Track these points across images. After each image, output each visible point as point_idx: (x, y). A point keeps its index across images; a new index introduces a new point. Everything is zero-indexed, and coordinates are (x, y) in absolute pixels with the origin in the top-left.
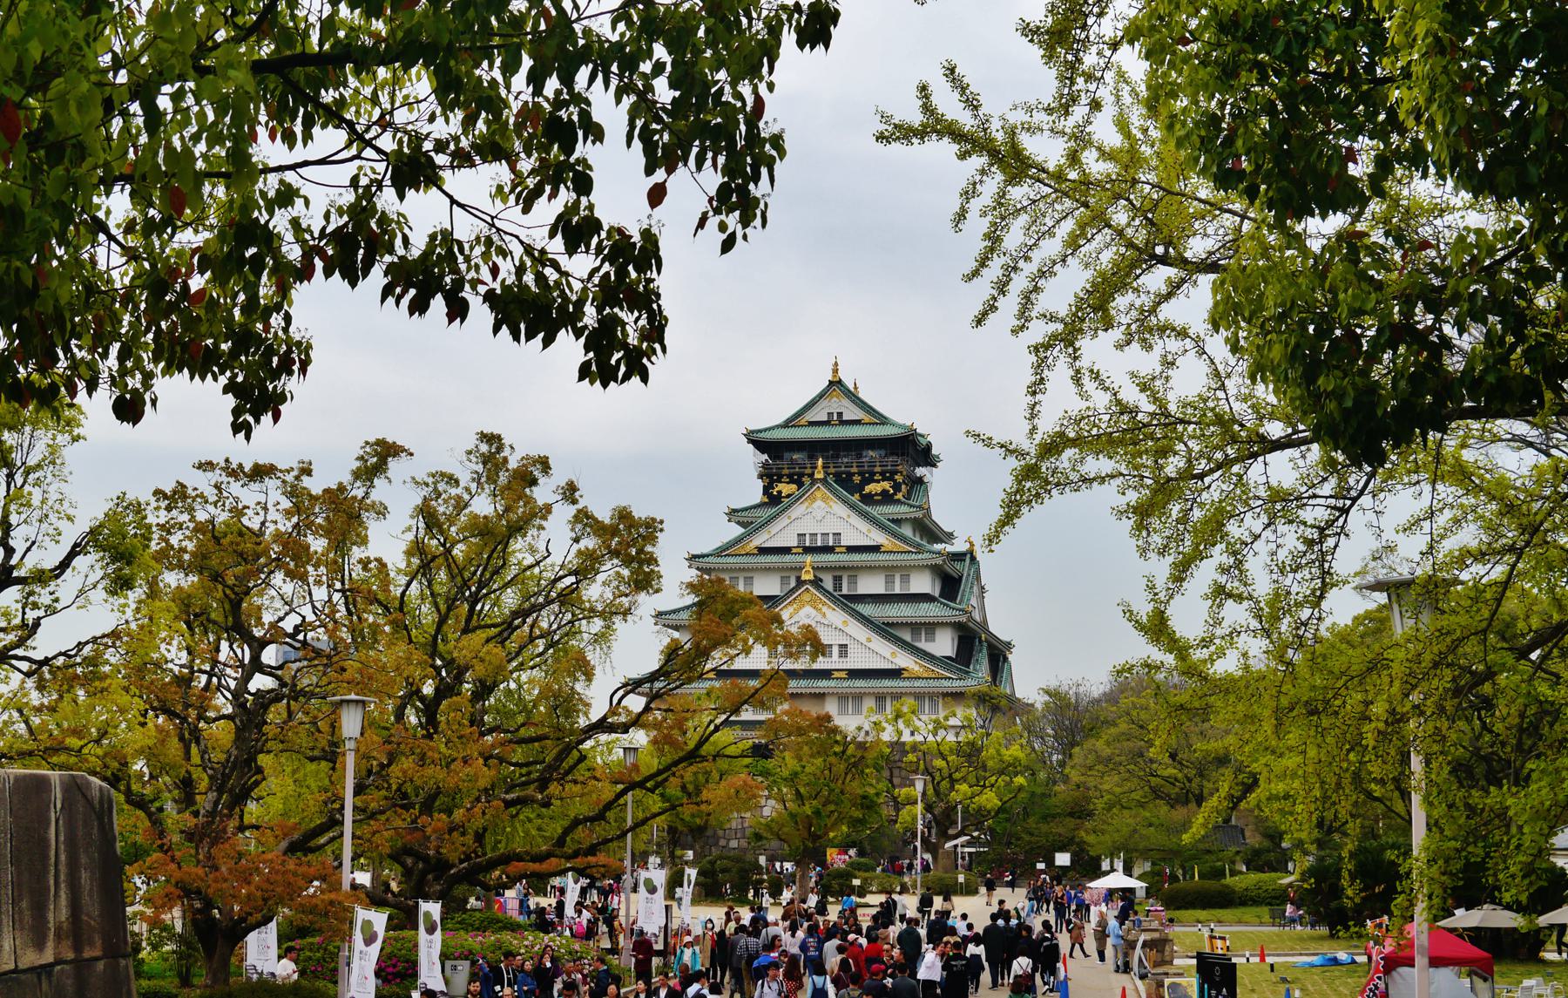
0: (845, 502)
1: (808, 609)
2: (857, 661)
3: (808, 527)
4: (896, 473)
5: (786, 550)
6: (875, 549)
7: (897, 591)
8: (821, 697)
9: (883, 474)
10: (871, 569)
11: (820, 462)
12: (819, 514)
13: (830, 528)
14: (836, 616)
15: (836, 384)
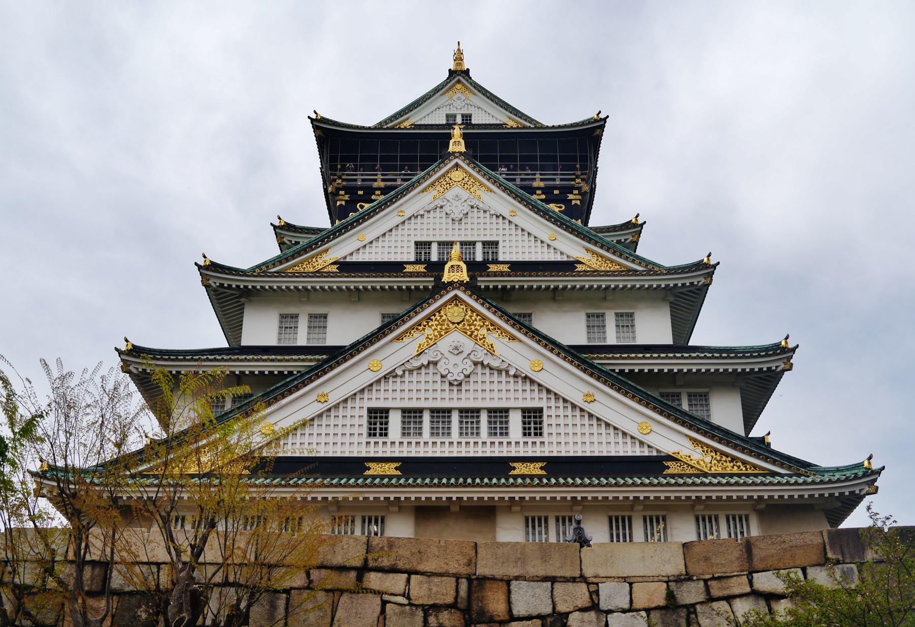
0: (505, 189)
1: (456, 337)
2: (565, 439)
3: (435, 230)
4: (570, 190)
5: (395, 268)
6: (568, 267)
7: (612, 339)
8: (486, 513)
9: (547, 190)
10: (556, 298)
11: (457, 132)
12: (457, 210)
13: (479, 230)
14: (518, 353)
15: (459, 75)
